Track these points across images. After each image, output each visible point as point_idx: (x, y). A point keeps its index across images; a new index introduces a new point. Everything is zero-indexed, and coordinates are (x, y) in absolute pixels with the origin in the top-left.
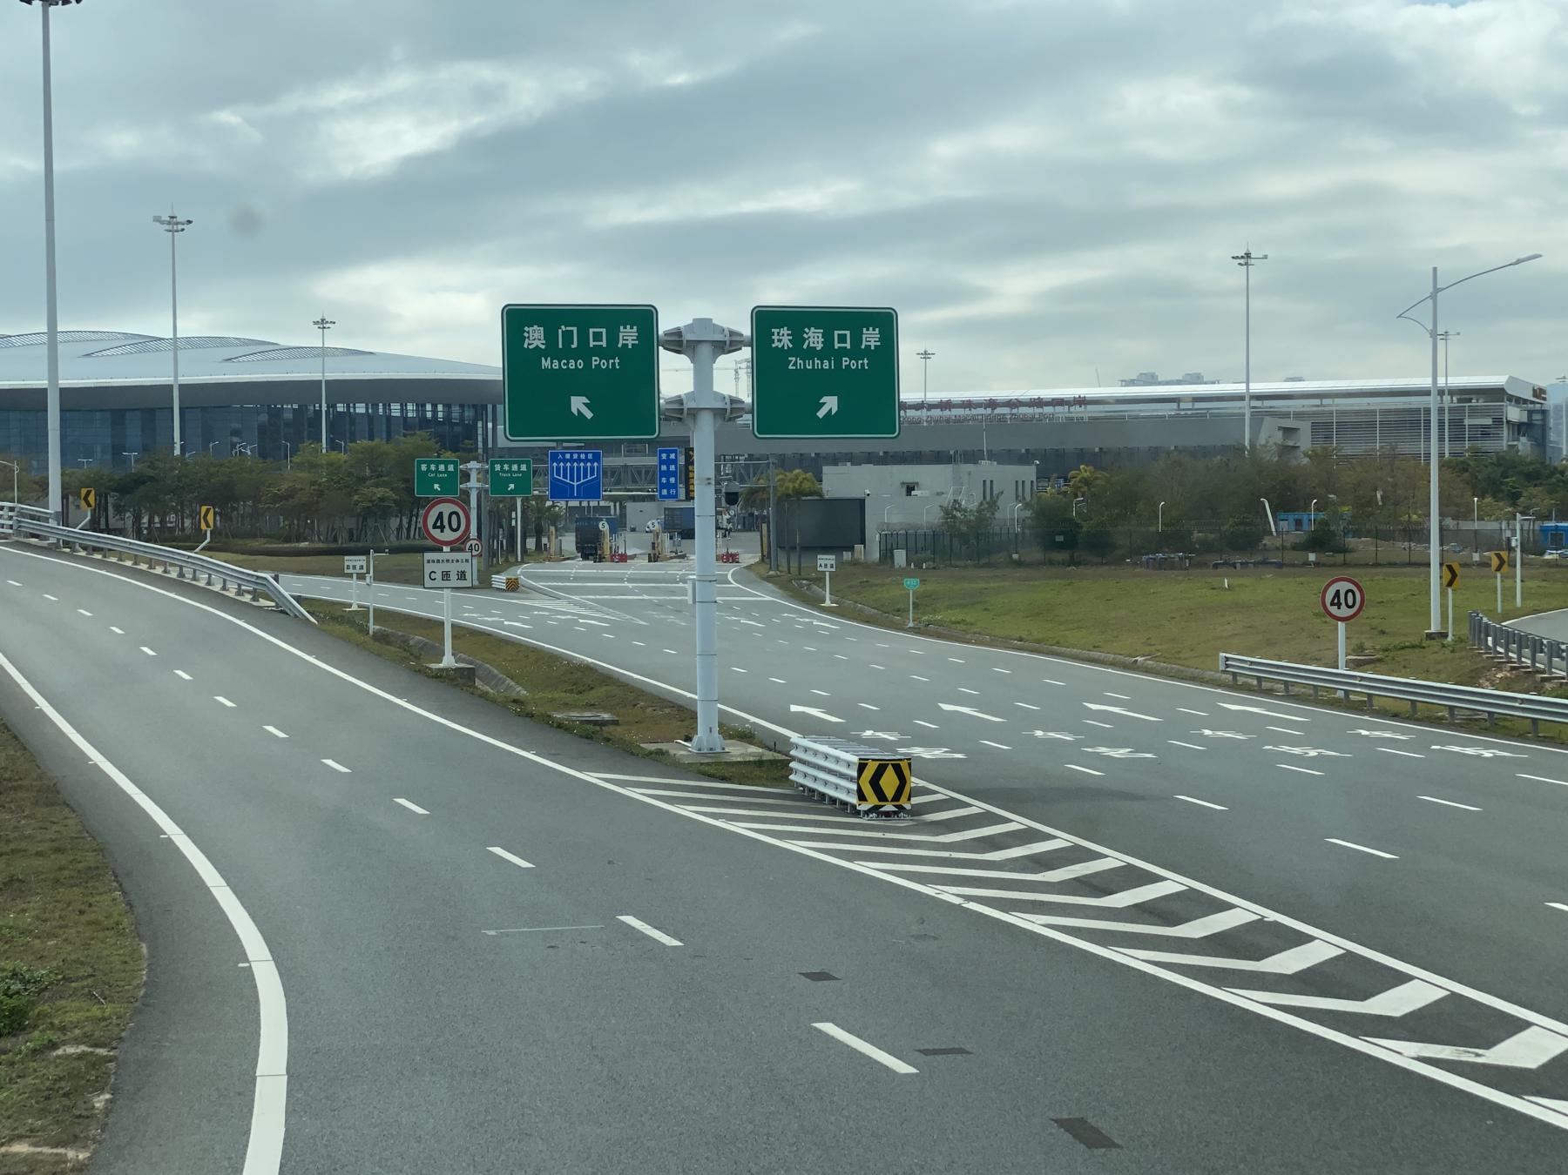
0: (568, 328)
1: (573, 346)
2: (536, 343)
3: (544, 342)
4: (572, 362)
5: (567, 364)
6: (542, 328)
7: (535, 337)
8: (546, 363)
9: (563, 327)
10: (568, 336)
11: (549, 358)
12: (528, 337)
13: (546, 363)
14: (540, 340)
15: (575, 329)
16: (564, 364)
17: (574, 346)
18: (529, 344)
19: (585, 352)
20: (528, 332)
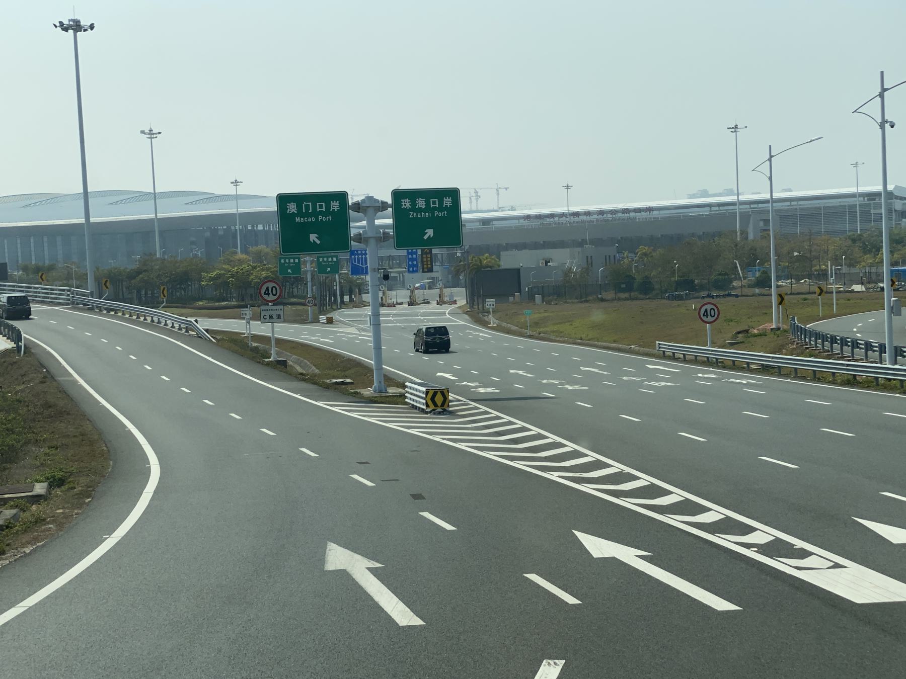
0: (307, 203)
2: (293, 211)
4: (310, 218)
7: (292, 208)
8: (298, 220)
9: (305, 203)
11: (299, 218)
13: (298, 220)
19: (315, 214)
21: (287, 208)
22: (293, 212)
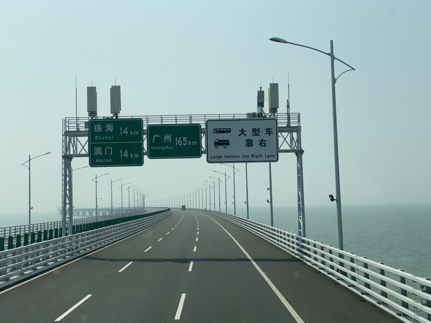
0: (109, 148)
2: (98, 153)
3: (102, 152)
5: (105, 161)
6: (101, 148)
9: (107, 148)
12: (96, 151)
14: (100, 152)
15: (111, 148)
16: (104, 161)
17: (111, 154)
18: (96, 154)
20: (96, 149)
21: (95, 151)
22: (99, 154)
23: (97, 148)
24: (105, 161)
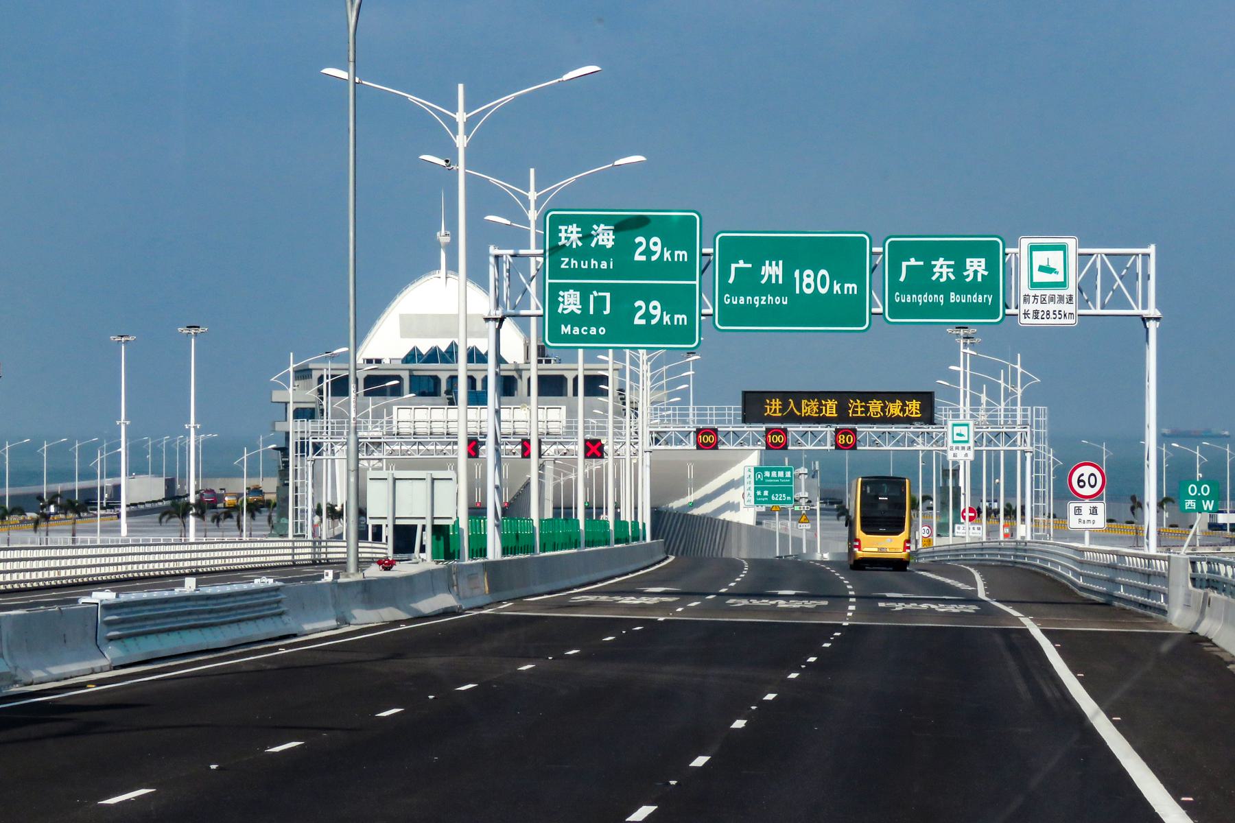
0: (600, 294)
1: (605, 313)
3: (580, 307)
6: (578, 293)
9: (595, 293)
10: (600, 302)
12: (563, 302)
16: (585, 331)
17: (607, 312)
18: (564, 309)
20: (563, 297)
23: (566, 293)
24: (586, 333)
